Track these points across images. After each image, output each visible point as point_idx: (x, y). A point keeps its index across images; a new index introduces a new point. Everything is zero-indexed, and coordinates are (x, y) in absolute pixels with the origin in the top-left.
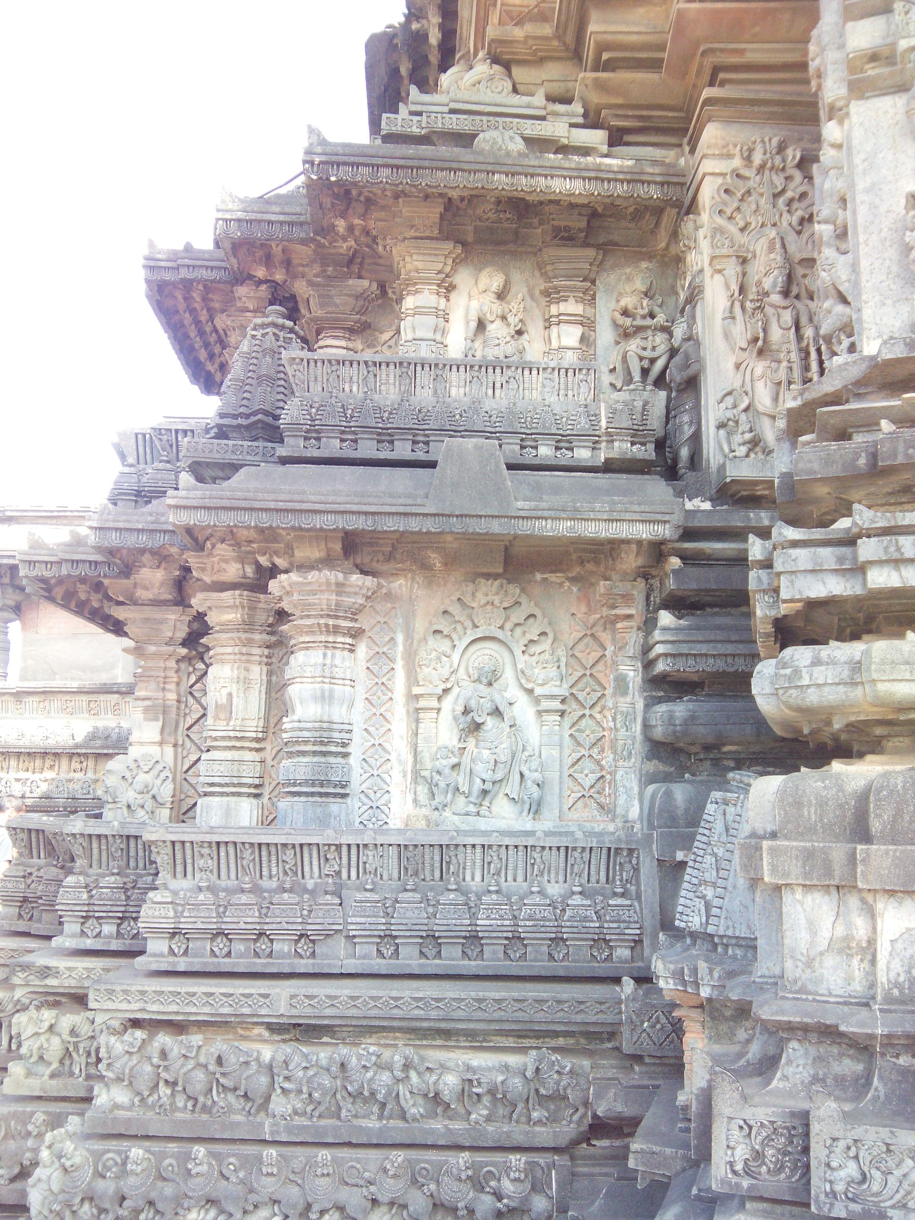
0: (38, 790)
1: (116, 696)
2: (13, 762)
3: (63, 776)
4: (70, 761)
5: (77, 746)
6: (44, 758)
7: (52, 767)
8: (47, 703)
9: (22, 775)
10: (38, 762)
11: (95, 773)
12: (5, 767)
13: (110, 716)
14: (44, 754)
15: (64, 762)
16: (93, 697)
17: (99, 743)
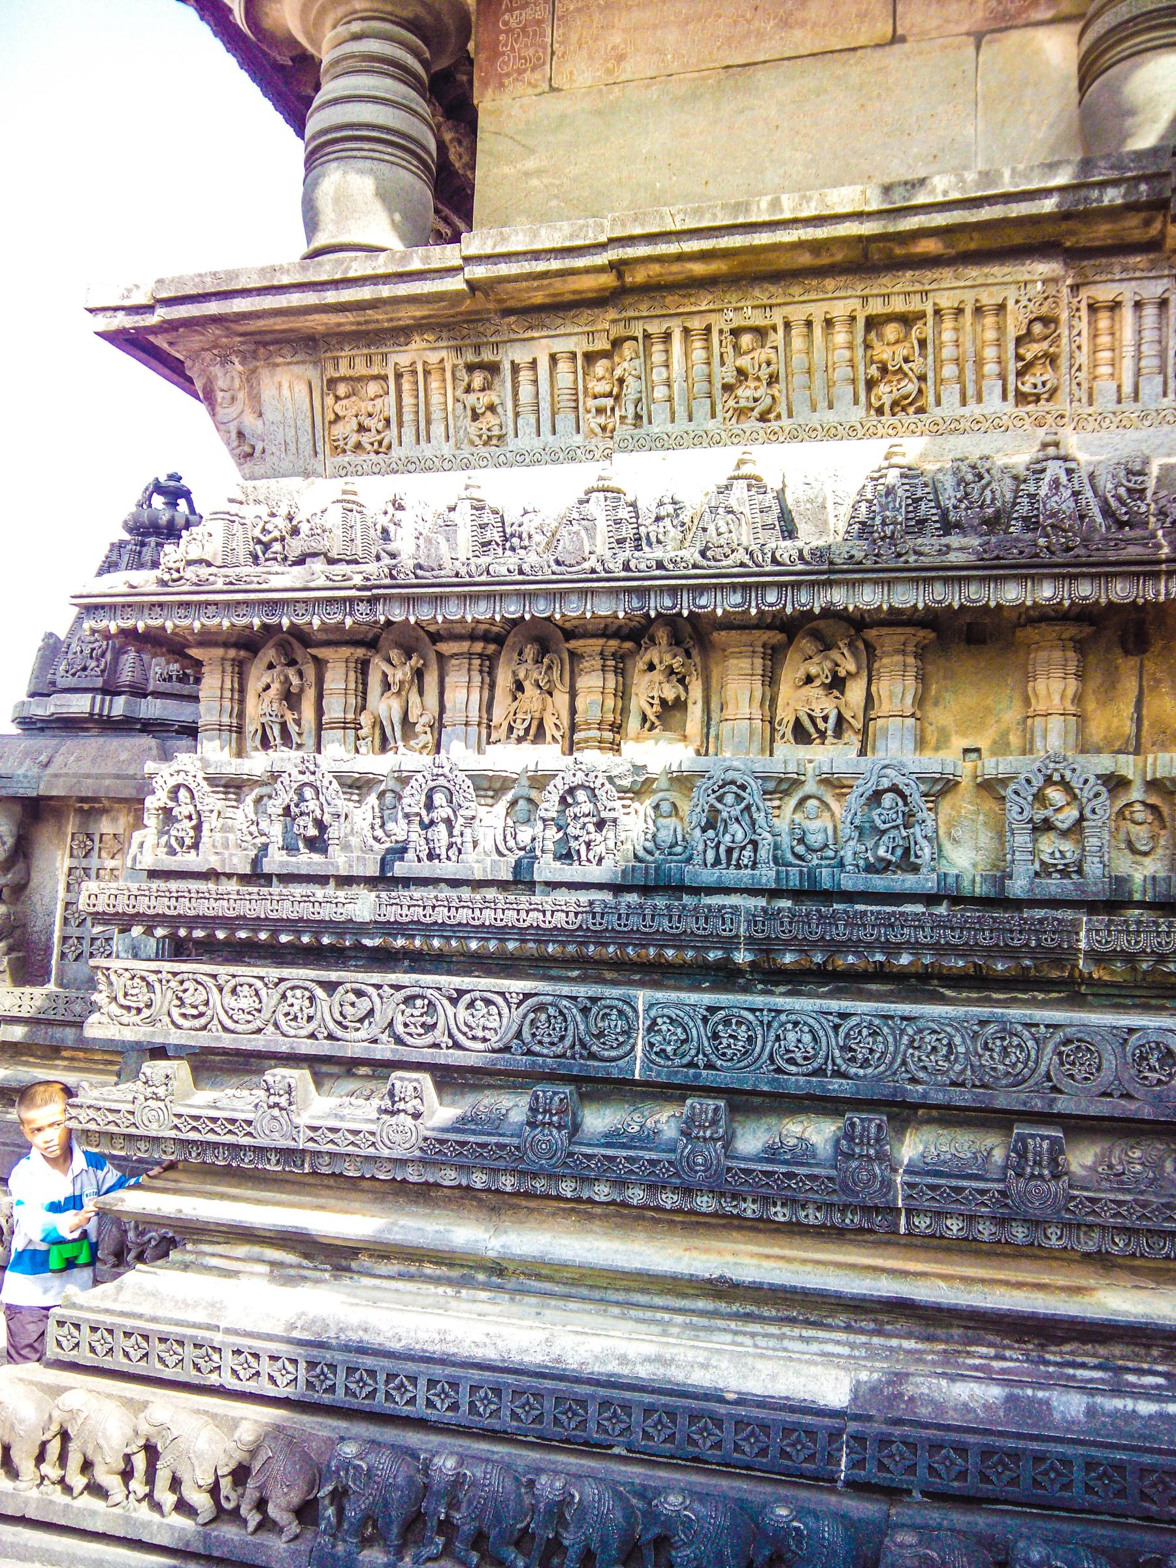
0: (603, 842)
1: (1044, 268)
2: (463, 693)
3: (739, 756)
4: (771, 679)
5: (825, 569)
6: (620, 665)
7: (670, 712)
8: (627, 363)
9: (510, 758)
10: (594, 688)
11: (921, 743)
12: (422, 715)
13: (993, 403)
14: (629, 638)
15: (740, 687)
16: (896, 293)
17: (962, 548)
